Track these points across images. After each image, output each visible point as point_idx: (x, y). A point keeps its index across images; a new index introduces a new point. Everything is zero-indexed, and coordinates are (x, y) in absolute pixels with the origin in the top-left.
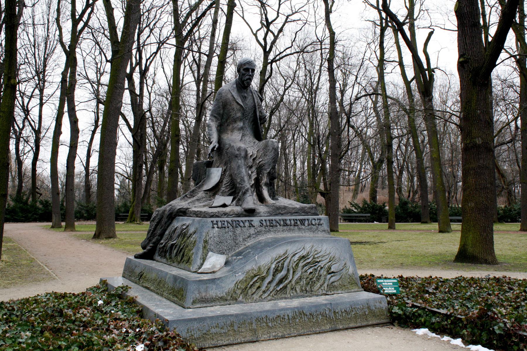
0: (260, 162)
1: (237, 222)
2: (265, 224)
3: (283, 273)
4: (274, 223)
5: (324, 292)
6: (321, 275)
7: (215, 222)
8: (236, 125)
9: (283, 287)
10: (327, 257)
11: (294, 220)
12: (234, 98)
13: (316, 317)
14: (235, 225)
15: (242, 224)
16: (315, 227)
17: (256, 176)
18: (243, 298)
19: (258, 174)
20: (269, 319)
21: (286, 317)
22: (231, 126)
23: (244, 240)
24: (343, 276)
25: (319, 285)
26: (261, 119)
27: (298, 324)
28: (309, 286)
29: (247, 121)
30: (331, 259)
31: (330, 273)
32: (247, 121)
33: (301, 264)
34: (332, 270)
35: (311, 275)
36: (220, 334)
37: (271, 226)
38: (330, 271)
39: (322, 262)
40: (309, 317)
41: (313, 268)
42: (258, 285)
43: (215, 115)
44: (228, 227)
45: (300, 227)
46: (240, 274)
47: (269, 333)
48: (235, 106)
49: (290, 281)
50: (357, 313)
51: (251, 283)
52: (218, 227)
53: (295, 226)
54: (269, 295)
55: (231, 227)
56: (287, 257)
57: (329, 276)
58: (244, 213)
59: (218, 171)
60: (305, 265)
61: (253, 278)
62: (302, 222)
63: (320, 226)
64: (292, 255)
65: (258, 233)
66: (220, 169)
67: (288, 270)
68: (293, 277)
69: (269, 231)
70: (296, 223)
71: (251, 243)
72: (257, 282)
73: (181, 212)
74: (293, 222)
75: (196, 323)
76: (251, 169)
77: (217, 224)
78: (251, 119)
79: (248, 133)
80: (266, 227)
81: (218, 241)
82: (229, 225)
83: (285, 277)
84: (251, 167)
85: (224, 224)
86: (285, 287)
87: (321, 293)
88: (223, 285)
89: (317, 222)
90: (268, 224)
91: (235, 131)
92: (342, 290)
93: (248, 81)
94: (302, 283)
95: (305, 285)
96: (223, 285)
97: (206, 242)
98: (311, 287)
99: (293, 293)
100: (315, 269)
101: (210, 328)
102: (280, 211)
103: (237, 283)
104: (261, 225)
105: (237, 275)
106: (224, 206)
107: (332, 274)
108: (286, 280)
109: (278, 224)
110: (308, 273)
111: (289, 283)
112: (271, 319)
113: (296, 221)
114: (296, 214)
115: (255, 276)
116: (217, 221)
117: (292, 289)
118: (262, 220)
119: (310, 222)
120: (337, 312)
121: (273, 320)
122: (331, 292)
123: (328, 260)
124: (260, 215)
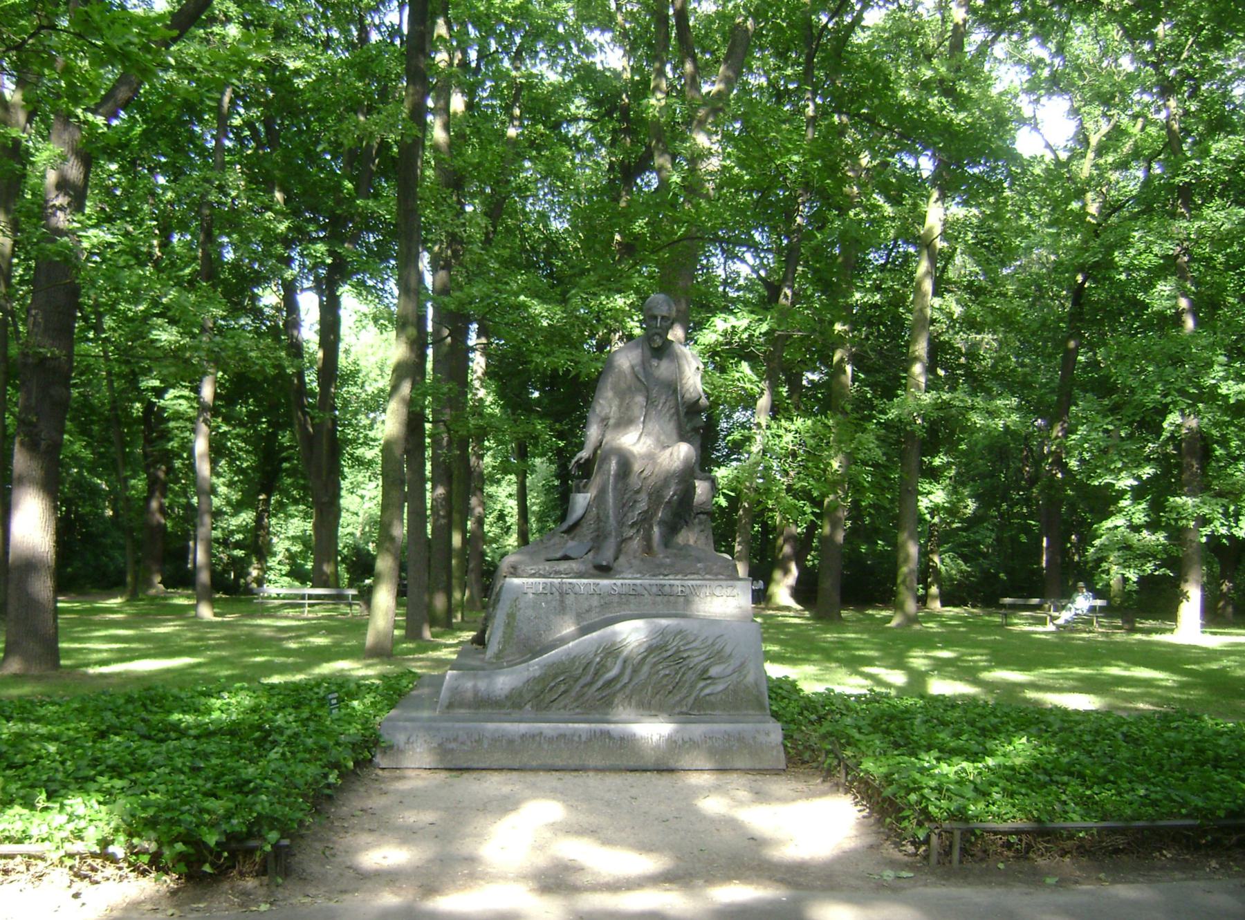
5: (684, 709)
21: (576, 738)
42: (562, 688)
49: (625, 686)
57: (702, 684)
68: (631, 680)
83: (615, 679)
97: (511, 616)
115: (563, 673)
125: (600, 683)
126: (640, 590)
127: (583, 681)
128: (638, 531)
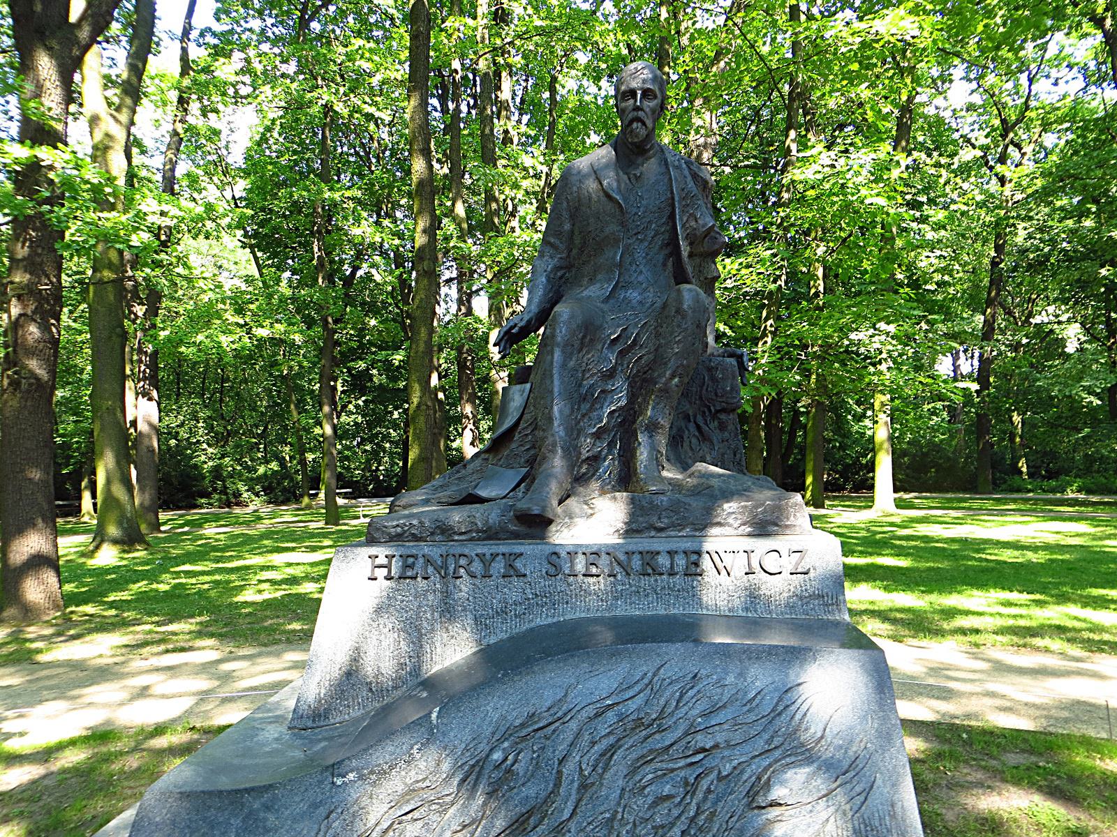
0: (640, 358)
11: (685, 552)
15: (477, 567)
17: (623, 402)
19: (632, 398)
30: (776, 742)
35: (663, 809)
39: (726, 753)
52: (388, 578)
64: (591, 711)
74: (681, 562)
78: (659, 241)
79: (641, 278)
82: (430, 570)
84: (611, 375)
104: (552, 570)
110: (650, 800)
123: (760, 745)
128: (611, 445)
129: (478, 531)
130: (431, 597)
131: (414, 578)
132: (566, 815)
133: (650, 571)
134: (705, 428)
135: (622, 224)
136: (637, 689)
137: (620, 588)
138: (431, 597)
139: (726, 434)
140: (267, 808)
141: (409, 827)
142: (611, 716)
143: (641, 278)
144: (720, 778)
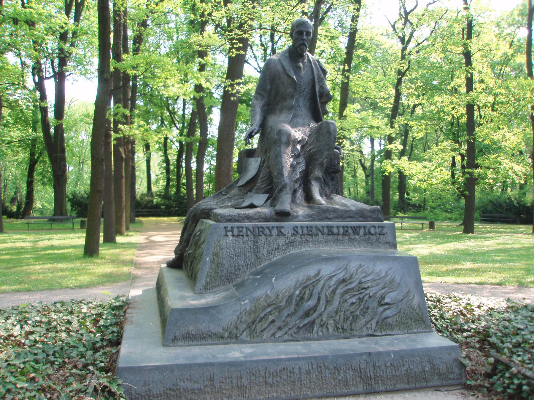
0: (310, 150)
1: (261, 229)
2: (300, 231)
3: (312, 303)
4: (314, 230)
5: (370, 332)
6: (368, 308)
7: (229, 229)
8: (285, 104)
9: (308, 323)
10: (380, 281)
12: (284, 70)
13: (344, 372)
14: (258, 232)
15: (267, 232)
16: (374, 238)
17: (304, 168)
18: (247, 336)
19: (308, 165)
20: (269, 373)
21: (297, 371)
22: (280, 105)
23: (269, 252)
24: (403, 310)
25: (363, 321)
26: (321, 96)
27: (314, 382)
28: (349, 322)
29: (302, 98)
31: (382, 305)
32: (302, 98)
33: (339, 291)
34: (387, 300)
35: (353, 307)
36: (192, 390)
37: (310, 235)
38: (382, 302)
39: (371, 289)
40: (333, 371)
41: (357, 297)
42: (271, 318)
43: (262, 92)
44: (248, 236)
45: (352, 236)
46: (247, 301)
47: (267, 392)
48: (285, 79)
49: (321, 315)
50: (410, 369)
51: (262, 315)
52: (233, 236)
53: (344, 235)
54: (286, 333)
55: (251, 236)
56: (319, 280)
57: (381, 309)
58: (275, 217)
59: (257, 161)
60: (346, 292)
61: (264, 309)
62: (356, 230)
63: (382, 237)
64: (327, 277)
65: (291, 244)
66: (259, 159)
67: (319, 299)
68: (325, 309)
69: (307, 241)
70: (347, 231)
71: (279, 257)
72: (271, 314)
73: (204, 213)
74: (341, 230)
75: (157, 373)
76: (298, 159)
77: (232, 230)
79: (302, 113)
80: (303, 237)
81: (232, 254)
82: (249, 233)
83: (314, 309)
85: (241, 231)
86: (313, 322)
87: (365, 332)
88: (220, 316)
89: (378, 230)
90: (305, 232)
91: (285, 111)
92: (400, 329)
93: (302, 47)
94: (337, 318)
95: (342, 320)
96: (220, 316)
97: (216, 254)
98: (351, 324)
99: (322, 332)
100: (360, 298)
101: (179, 380)
102: (327, 215)
103: (241, 314)
104: (296, 233)
105: (242, 303)
106: (252, 206)
107: (386, 307)
108: (315, 312)
109: (319, 233)
110: (349, 304)
111: (317, 318)
112: (273, 373)
113: (346, 229)
114: (349, 219)
115: (269, 305)
116: (231, 227)
117: (321, 326)
118: (297, 227)
119: (367, 231)
120: (379, 367)
121: (275, 374)
122: (381, 332)
123: (381, 285)
124: (298, 219)
125: (301, 313)
126: (314, 230)
127: (285, 313)
128: (300, 186)
129: (262, 218)
130: (249, 243)
131: (243, 236)
132: (323, 310)
133: (331, 233)
134: (326, 179)
135: (295, 89)
136: (341, 270)
137: (320, 240)
138: (249, 243)
139: (334, 183)
140: (218, 313)
141: (270, 317)
142: (334, 279)
143: (302, 113)
144: (370, 297)
